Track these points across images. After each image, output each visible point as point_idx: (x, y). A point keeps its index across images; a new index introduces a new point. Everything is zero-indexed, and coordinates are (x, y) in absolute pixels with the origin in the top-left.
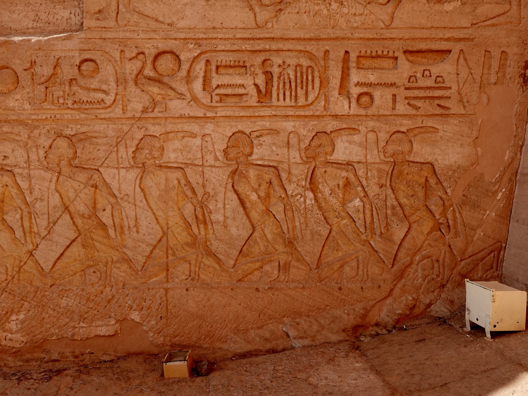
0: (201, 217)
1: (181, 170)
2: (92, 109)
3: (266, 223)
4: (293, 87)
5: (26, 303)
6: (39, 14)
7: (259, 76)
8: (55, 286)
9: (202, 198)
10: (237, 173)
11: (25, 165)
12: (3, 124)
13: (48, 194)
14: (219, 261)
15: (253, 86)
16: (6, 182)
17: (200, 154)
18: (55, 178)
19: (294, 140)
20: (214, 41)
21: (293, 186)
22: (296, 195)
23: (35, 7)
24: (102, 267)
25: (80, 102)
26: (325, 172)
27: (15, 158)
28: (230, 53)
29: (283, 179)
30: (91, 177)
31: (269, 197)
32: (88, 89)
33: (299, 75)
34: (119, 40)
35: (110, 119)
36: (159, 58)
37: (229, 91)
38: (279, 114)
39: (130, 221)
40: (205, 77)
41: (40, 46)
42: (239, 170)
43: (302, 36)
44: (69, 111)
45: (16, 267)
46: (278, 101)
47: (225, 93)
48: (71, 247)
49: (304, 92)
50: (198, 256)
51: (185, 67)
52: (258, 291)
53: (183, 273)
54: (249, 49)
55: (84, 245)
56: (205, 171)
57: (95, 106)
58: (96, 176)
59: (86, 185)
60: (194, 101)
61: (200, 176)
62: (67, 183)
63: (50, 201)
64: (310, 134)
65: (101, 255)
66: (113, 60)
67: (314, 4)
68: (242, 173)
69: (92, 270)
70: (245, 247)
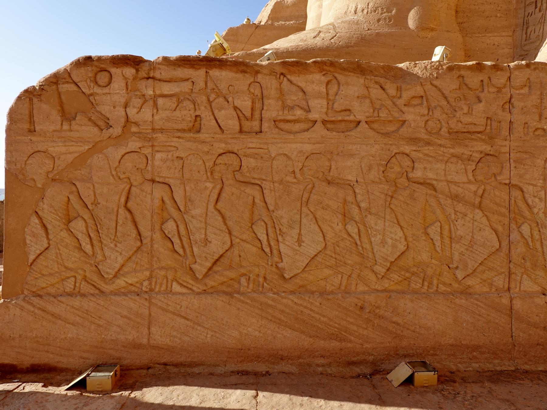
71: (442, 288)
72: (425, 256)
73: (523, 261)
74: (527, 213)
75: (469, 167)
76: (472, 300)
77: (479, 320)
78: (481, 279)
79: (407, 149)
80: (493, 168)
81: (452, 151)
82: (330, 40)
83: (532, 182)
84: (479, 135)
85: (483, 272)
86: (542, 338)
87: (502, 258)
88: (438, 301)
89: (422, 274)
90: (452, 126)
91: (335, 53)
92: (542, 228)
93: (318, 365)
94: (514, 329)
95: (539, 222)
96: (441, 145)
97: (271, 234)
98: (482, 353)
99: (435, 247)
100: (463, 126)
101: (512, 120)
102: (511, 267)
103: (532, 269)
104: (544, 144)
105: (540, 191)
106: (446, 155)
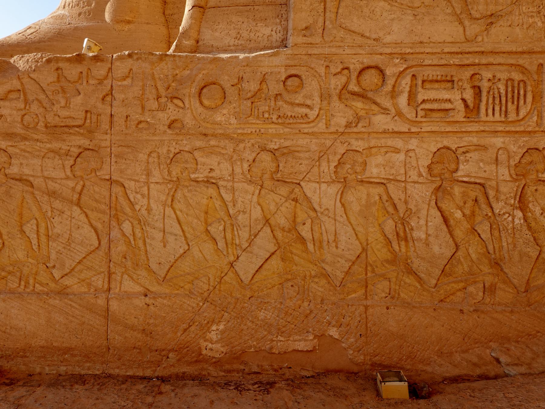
0: (402, 234)
1: (383, 185)
2: (296, 123)
3: (471, 242)
4: (504, 102)
5: (227, 314)
6: (241, 32)
7: (467, 91)
8: (253, 298)
9: (404, 214)
10: (441, 190)
11: (229, 178)
12: (210, 138)
13: (251, 207)
14: (419, 279)
15: (461, 101)
16: (211, 194)
17: (404, 170)
18: (258, 191)
19: (503, 157)
20: (420, 56)
21: (501, 204)
22: (504, 214)
23: (237, 25)
24: (300, 281)
26: (536, 190)
27: (221, 171)
28: (437, 68)
29: (490, 197)
30: (293, 191)
31: (474, 215)
32: (292, 104)
33: (510, 89)
34: (324, 56)
35: (313, 134)
36: (363, 73)
37: (435, 106)
38: (487, 129)
39: (329, 236)
40: (410, 91)
41: (248, 63)
42: (443, 186)
43: (514, 50)
44: (273, 126)
45: (218, 277)
46: (487, 116)
47: (431, 108)
48: (270, 259)
49: (515, 107)
50: (398, 274)
51: (390, 82)
52: (463, 313)
53: (383, 291)
54: (457, 63)
55: (282, 259)
56: (408, 187)
57: (299, 121)
58: (297, 190)
59: (287, 199)
60: (399, 116)
61: (403, 192)
62: (269, 196)
63: (252, 214)
64: (520, 150)
65: (299, 269)
66: (317, 75)
67: (528, 16)
68: (446, 189)
69: (290, 284)
70: (447, 266)
71: (38, 288)
72: (21, 255)
73: (124, 260)
74: (128, 210)
75: (67, 162)
76: (66, 300)
77: (71, 322)
78: (79, 279)
80: (93, 163)
81: (48, 146)
82: (28, 35)
83: (134, 178)
84: (77, 129)
85: (81, 271)
86: (139, 341)
87: (101, 257)
88: (30, 301)
89: (18, 274)
91: (25, 48)
92: (144, 224)
94: (109, 331)
95: (141, 219)
96: (38, 140)
98: (73, 355)
99: (32, 246)
100: (61, 120)
101: (112, 113)
102: (111, 266)
103: (134, 268)
104: (148, 137)
105: (142, 187)
106: (43, 150)
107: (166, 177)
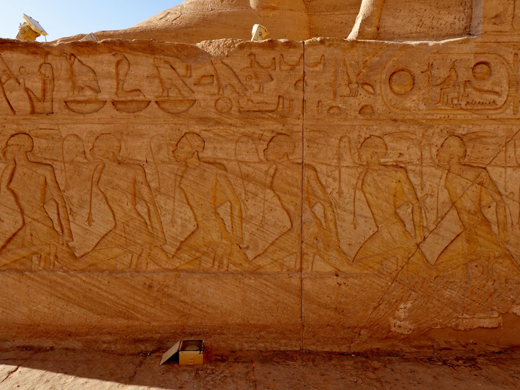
2: (483, 110)
5: (414, 293)
6: (423, 19)
8: (438, 278)
11: (418, 162)
12: (400, 123)
13: (438, 190)
16: (400, 178)
18: (445, 175)
23: (420, 12)
24: (484, 261)
25: (472, 103)
27: (410, 155)
30: (479, 175)
32: (480, 91)
34: (513, 43)
35: (500, 120)
39: (513, 218)
41: (438, 50)
44: (461, 112)
45: (405, 258)
48: (455, 241)
55: (468, 240)
57: (487, 107)
59: (473, 182)
62: (456, 180)
63: (439, 197)
65: (483, 250)
66: (505, 63)
69: (474, 264)
71: (232, 268)
72: (215, 236)
73: (315, 241)
74: (320, 193)
75: (260, 146)
76: (261, 280)
77: (267, 300)
79: (197, 129)
80: (285, 147)
81: (242, 130)
82: (173, 21)
83: (326, 162)
84: (270, 114)
85: (274, 252)
86: (332, 319)
87: (293, 239)
88: (226, 281)
89: (212, 254)
90: (242, 106)
91: (173, 34)
92: (336, 207)
93: (104, 342)
94: (303, 309)
95: (333, 202)
96: (231, 125)
97: (62, 214)
98: (270, 333)
99: (225, 227)
100: (254, 105)
101: (305, 99)
102: (303, 247)
103: (325, 249)
104: (339, 123)
105: (334, 170)
106: (236, 134)
107: (357, 161)
